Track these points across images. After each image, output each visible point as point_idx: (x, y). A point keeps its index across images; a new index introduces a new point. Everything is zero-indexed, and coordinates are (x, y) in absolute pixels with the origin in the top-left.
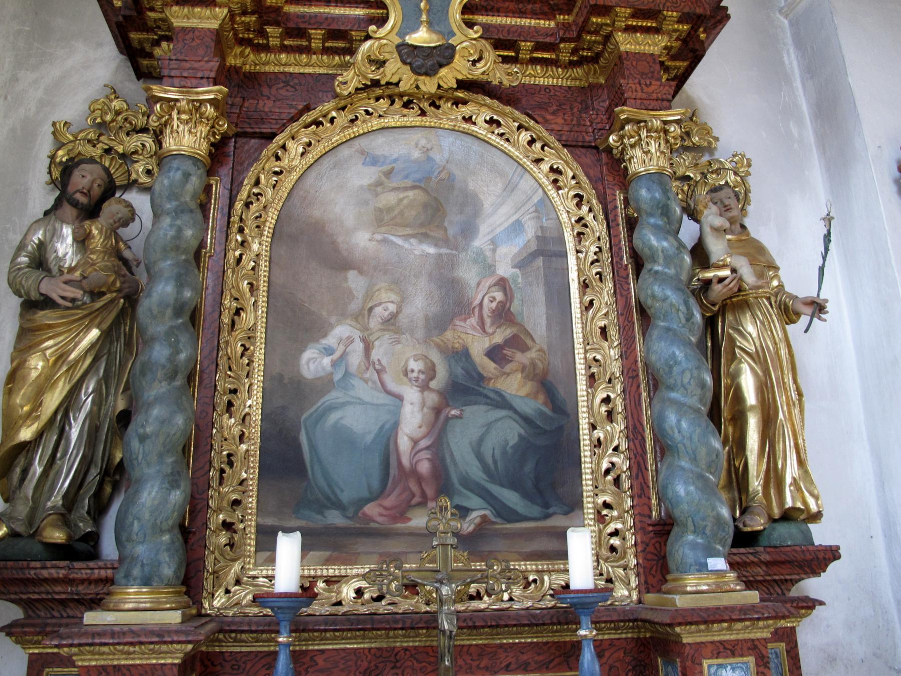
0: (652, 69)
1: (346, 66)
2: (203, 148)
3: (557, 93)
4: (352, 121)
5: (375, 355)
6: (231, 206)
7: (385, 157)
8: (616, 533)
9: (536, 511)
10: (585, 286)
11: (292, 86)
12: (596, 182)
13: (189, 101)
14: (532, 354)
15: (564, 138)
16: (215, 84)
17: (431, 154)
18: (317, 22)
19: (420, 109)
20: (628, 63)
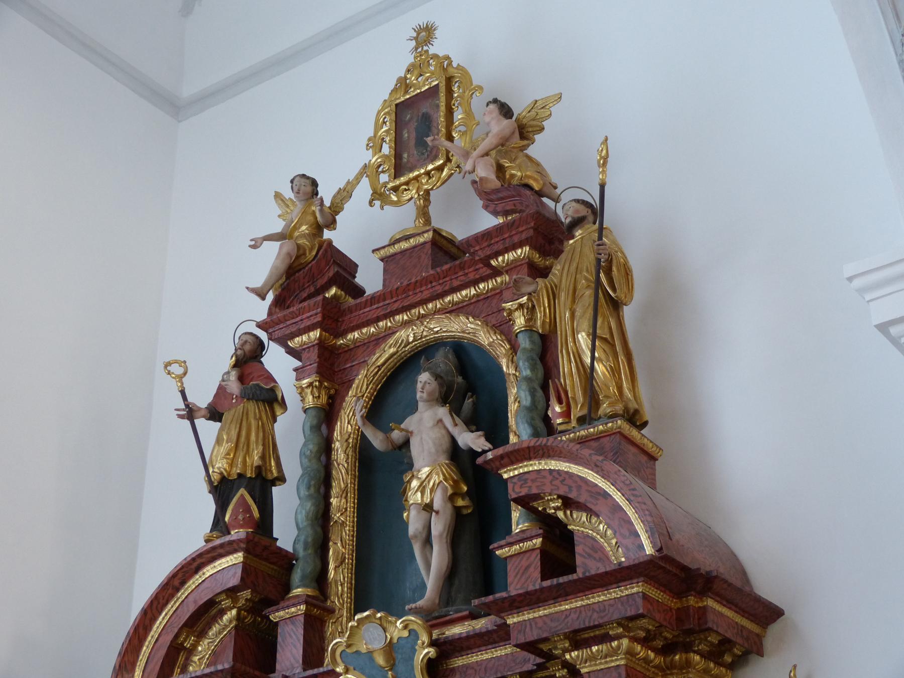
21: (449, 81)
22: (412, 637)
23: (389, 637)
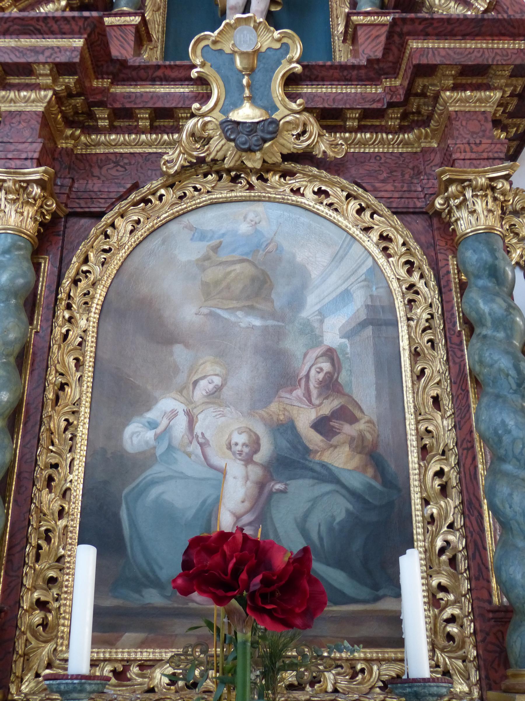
0: (483, 128)
1: (171, 144)
2: (30, 227)
3: (388, 161)
4: (181, 198)
5: (198, 429)
6: (59, 284)
7: (214, 232)
8: (452, 619)
9: (364, 592)
10: (416, 354)
11: (122, 166)
12: (428, 248)
13: (15, 182)
14: (361, 426)
15: (394, 205)
16: (39, 165)
17: (258, 227)
18: (143, 102)
19: (248, 183)
20: (457, 123)
22: (282, 50)
23: (259, 45)
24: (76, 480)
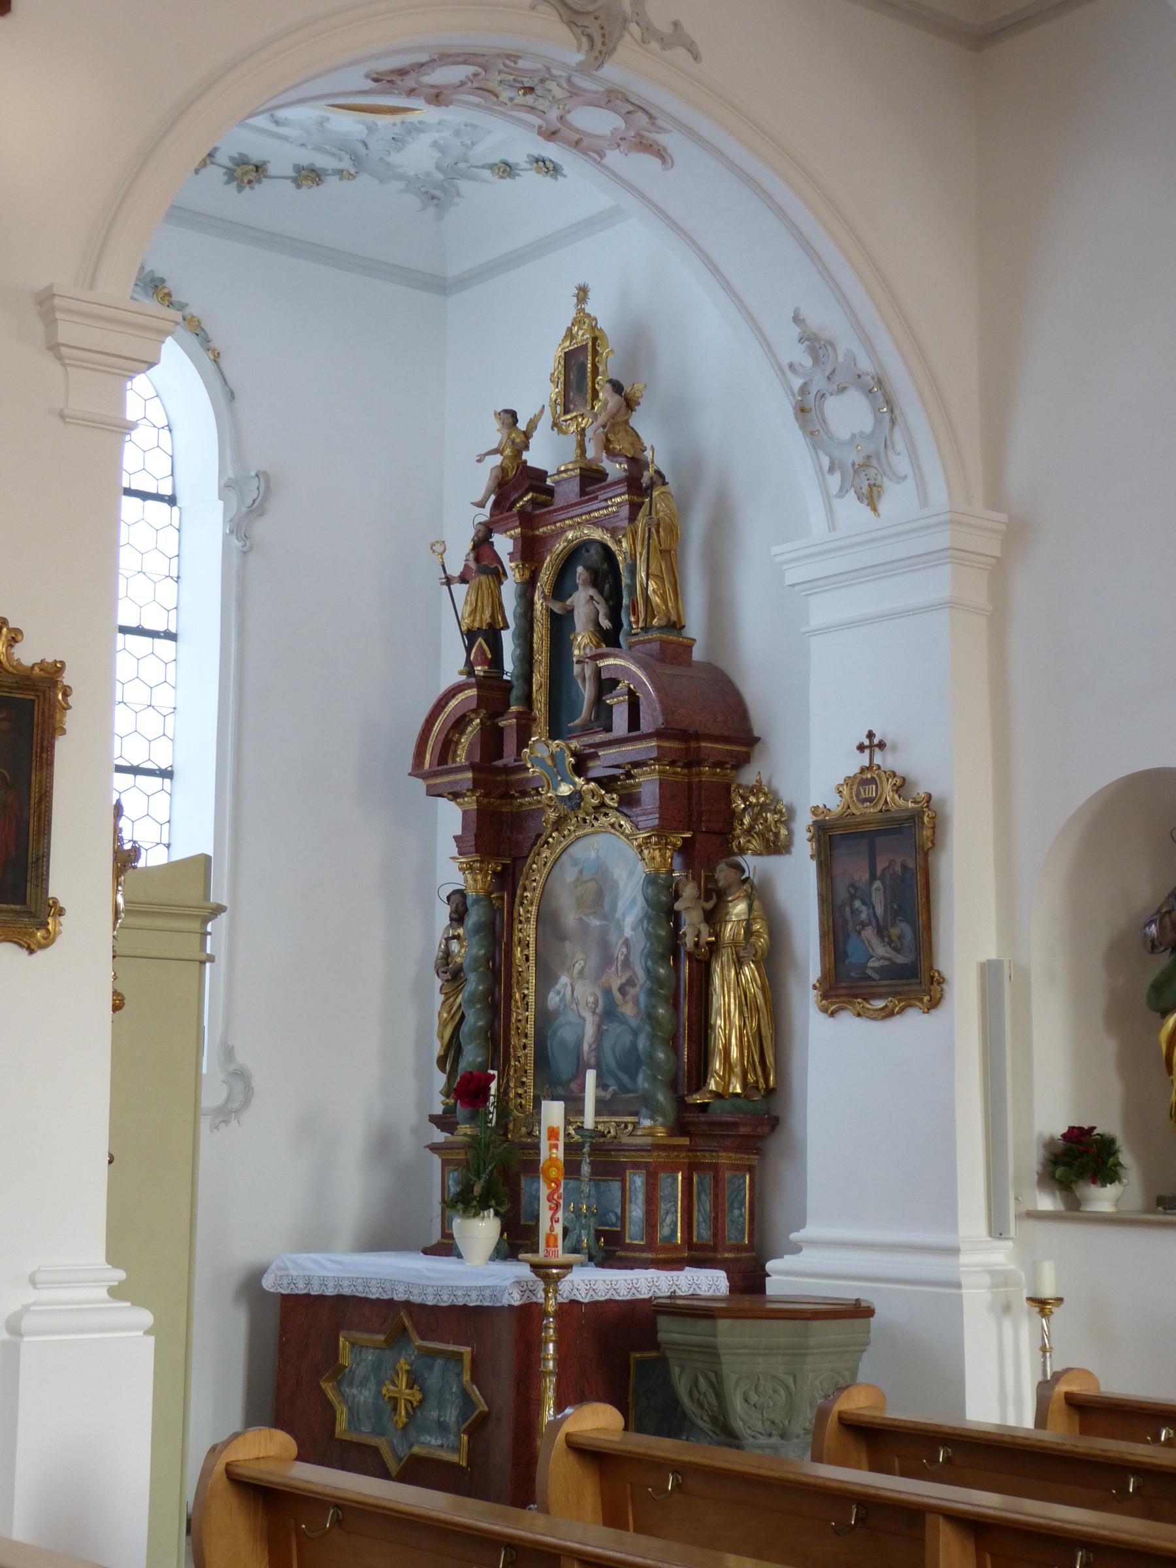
21: (595, 339)
24: (530, 1029)
